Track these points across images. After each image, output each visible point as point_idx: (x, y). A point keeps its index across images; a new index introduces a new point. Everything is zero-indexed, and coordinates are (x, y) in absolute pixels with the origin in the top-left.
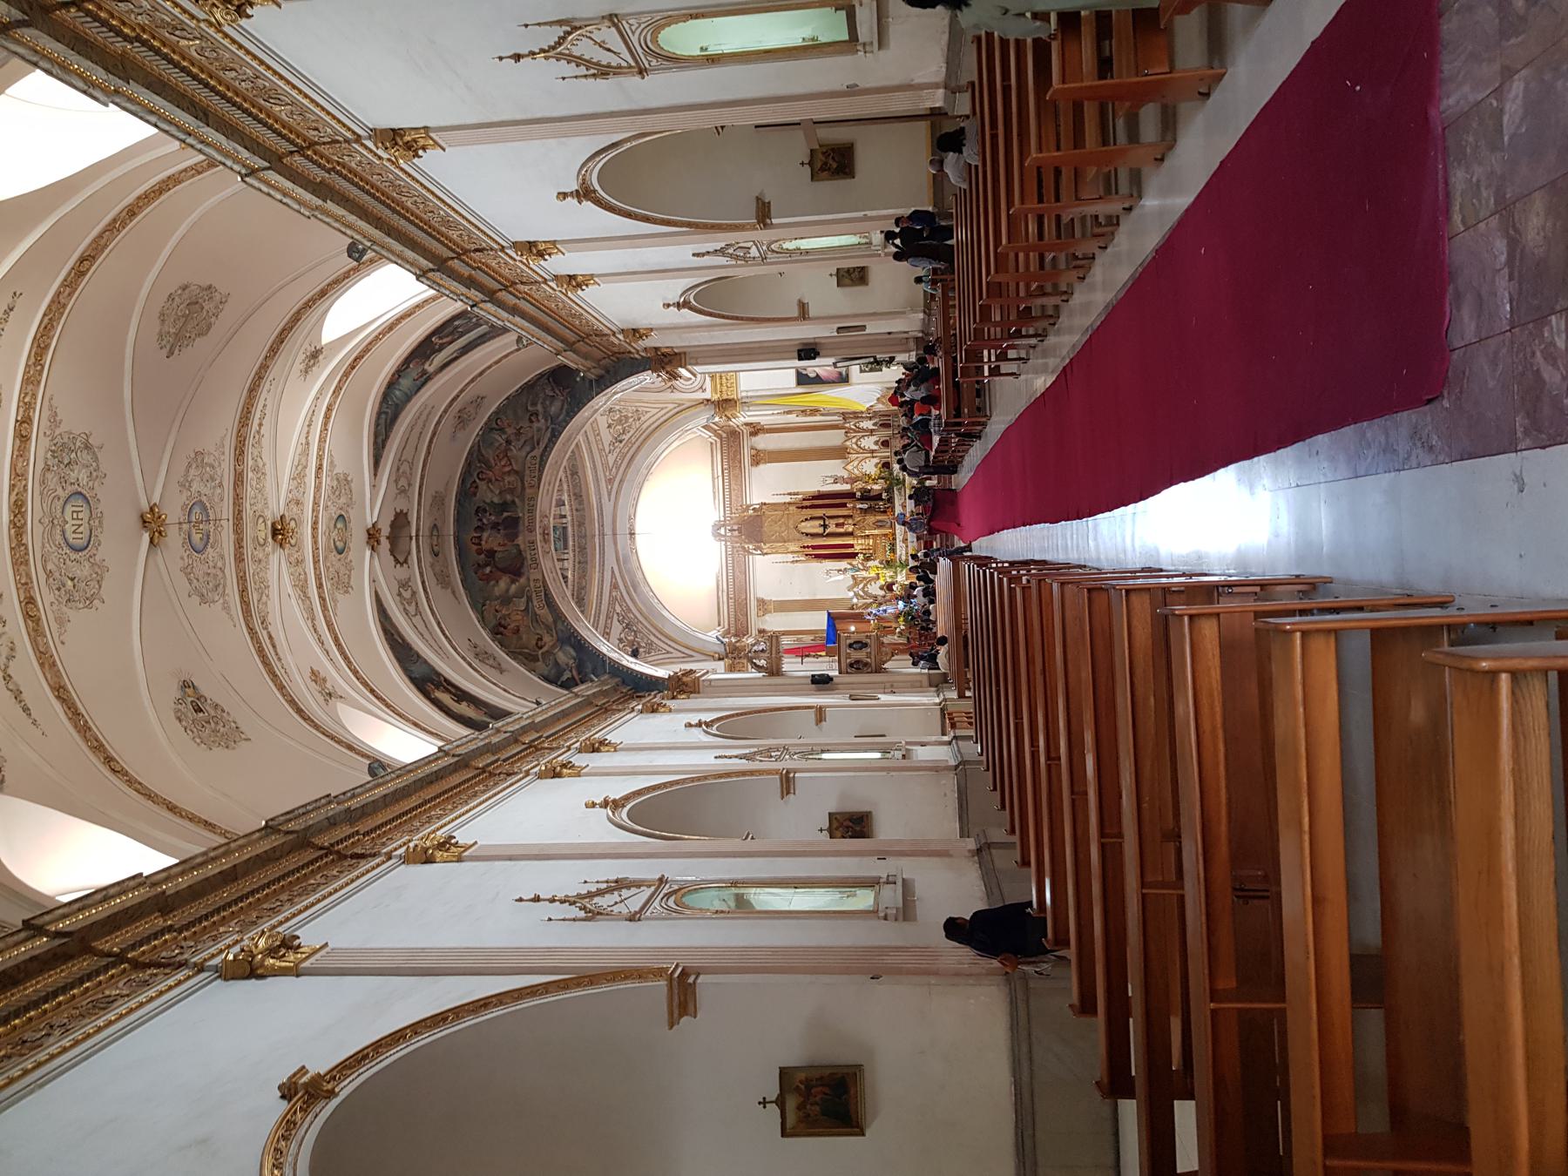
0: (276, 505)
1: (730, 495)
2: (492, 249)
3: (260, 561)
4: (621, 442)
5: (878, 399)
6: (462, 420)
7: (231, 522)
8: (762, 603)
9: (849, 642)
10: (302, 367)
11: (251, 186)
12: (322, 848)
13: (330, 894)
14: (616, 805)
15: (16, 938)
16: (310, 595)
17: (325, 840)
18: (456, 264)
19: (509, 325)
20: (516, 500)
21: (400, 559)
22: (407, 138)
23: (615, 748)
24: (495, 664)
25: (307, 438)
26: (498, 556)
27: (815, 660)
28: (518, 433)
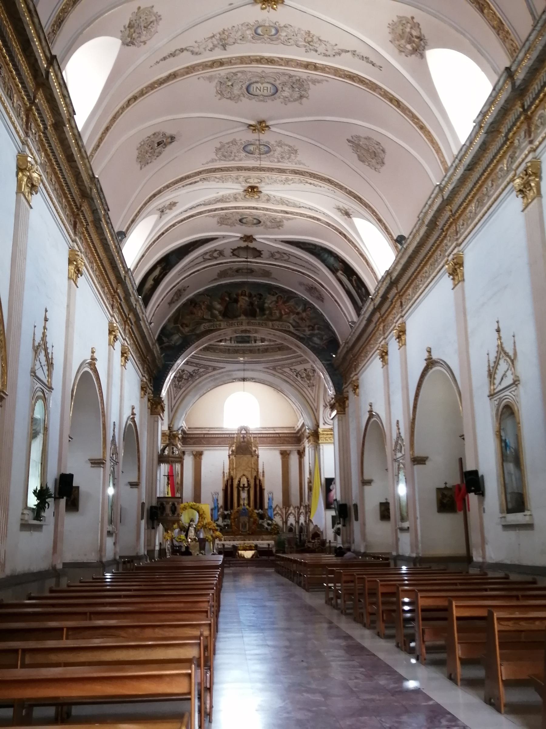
0: (266, 189)
1: (264, 437)
2: (402, 311)
3: (237, 179)
4: (297, 376)
5: (316, 526)
6: (311, 289)
7: (258, 166)
9: (176, 503)
10: (341, 207)
11: (434, 189)
13: (57, 210)
14: (92, 364)
15: (47, 52)
17: (85, 208)
19: (362, 317)
20: (265, 316)
21: (235, 252)
22: (458, 270)
23: (124, 366)
24: (174, 300)
26: (235, 305)
27: (166, 483)
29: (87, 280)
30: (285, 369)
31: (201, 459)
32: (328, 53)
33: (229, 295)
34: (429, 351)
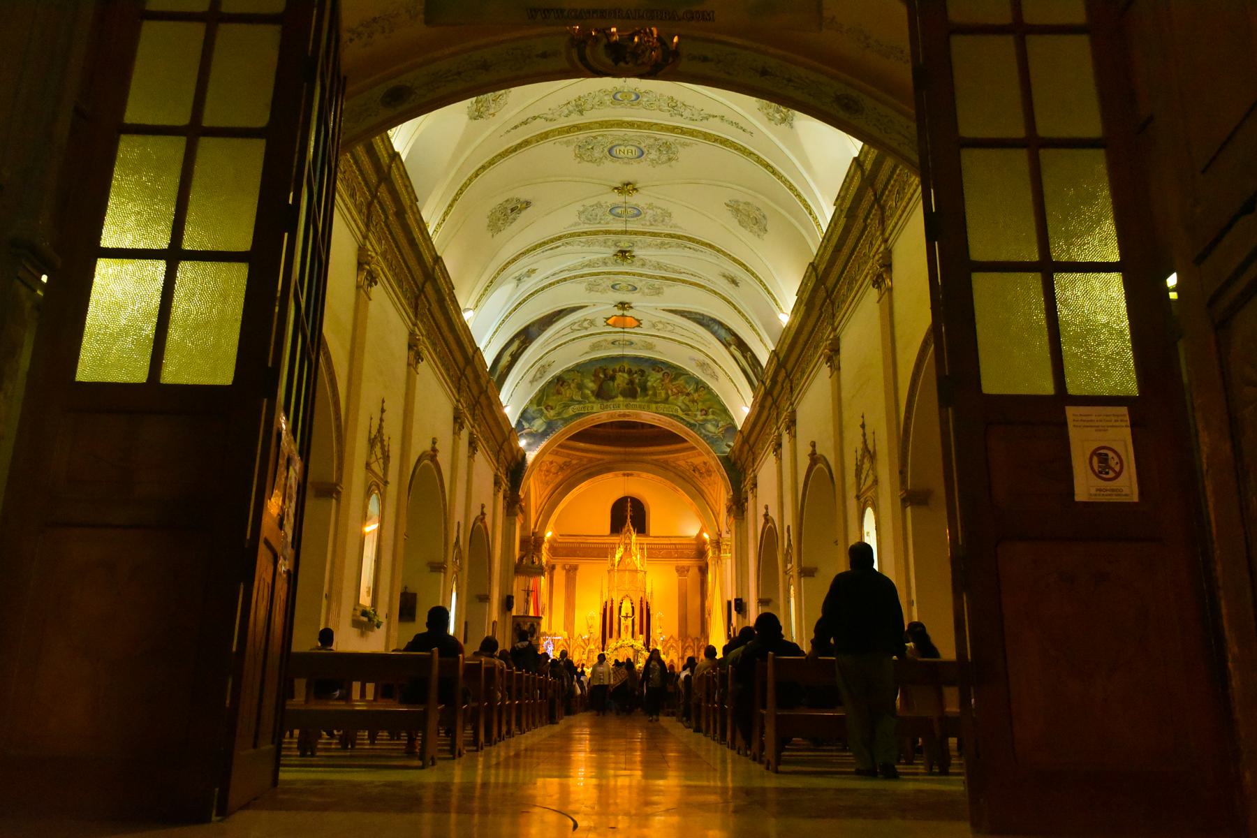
2: (792, 397)
3: (605, 243)
4: (694, 471)
6: (702, 365)
8: (575, 568)
9: (535, 624)
10: (727, 274)
12: (423, 287)
16: (585, 269)
17: (429, 288)
18: (783, 374)
20: (648, 397)
23: (471, 456)
25: (684, 273)
26: (611, 383)
28: (693, 401)
29: (430, 365)
30: (678, 462)
31: (575, 575)
32: (694, 118)
33: (605, 371)
34: (813, 445)
